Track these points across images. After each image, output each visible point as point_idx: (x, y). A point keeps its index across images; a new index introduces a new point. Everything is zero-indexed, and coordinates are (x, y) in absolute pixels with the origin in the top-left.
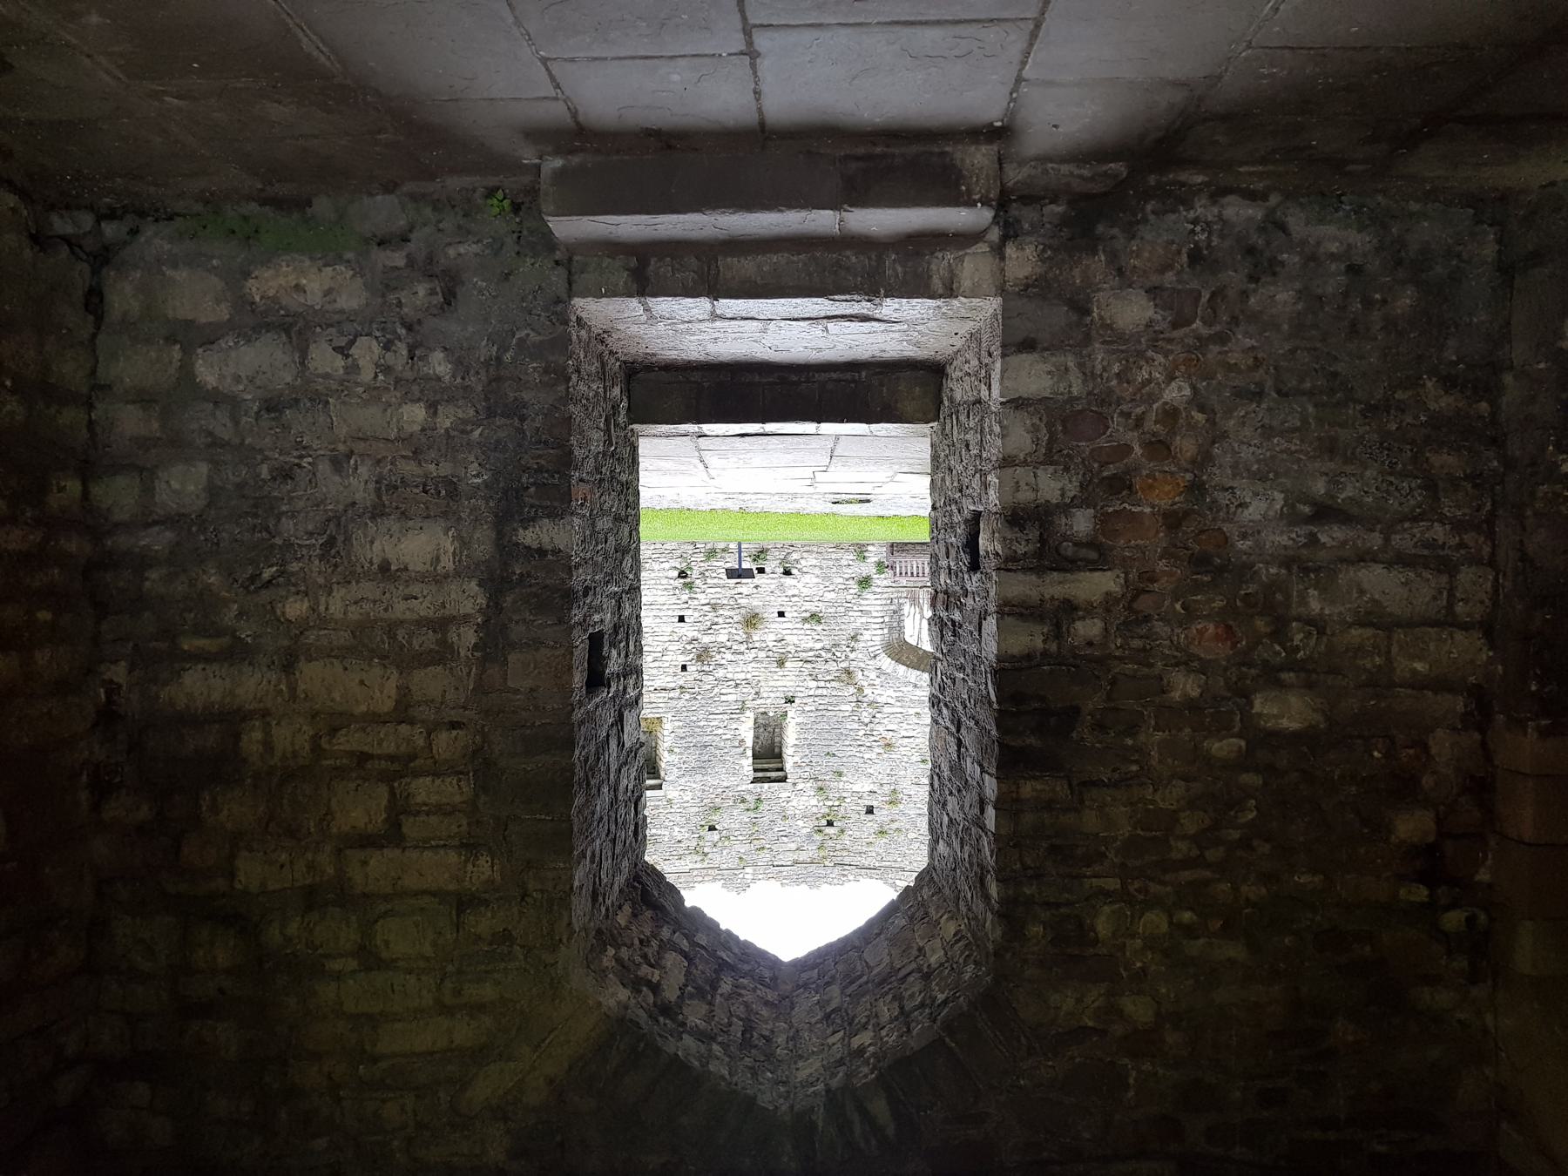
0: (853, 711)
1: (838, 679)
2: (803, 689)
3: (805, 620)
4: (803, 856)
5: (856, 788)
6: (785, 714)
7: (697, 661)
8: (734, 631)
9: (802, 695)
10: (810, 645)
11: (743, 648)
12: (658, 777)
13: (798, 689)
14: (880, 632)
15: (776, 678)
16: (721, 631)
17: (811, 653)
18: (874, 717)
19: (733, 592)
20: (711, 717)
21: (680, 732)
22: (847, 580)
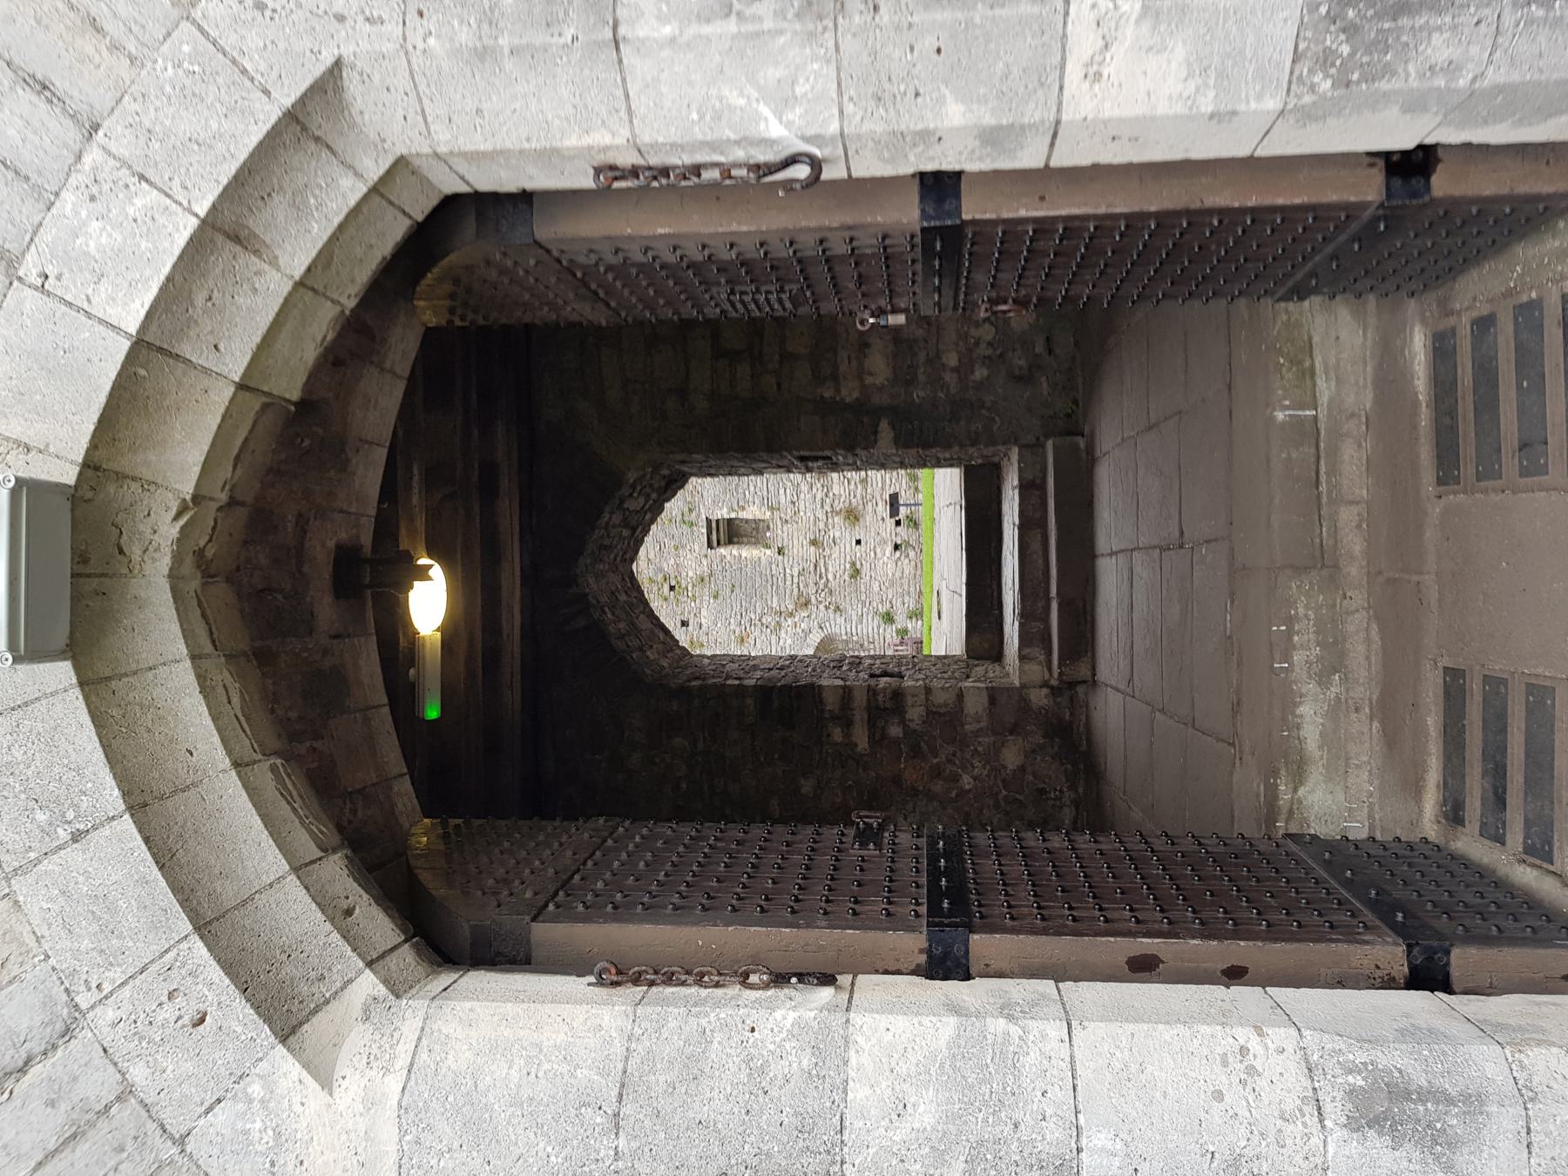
1: (800, 594)
3: (853, 564)
5: (704, 613)
6: (768, 547)
10: (830, 569)
13: (791, 559)
14: (843, 633)
15: (801, 538)
16: (842, 488)
17: (823, 570)
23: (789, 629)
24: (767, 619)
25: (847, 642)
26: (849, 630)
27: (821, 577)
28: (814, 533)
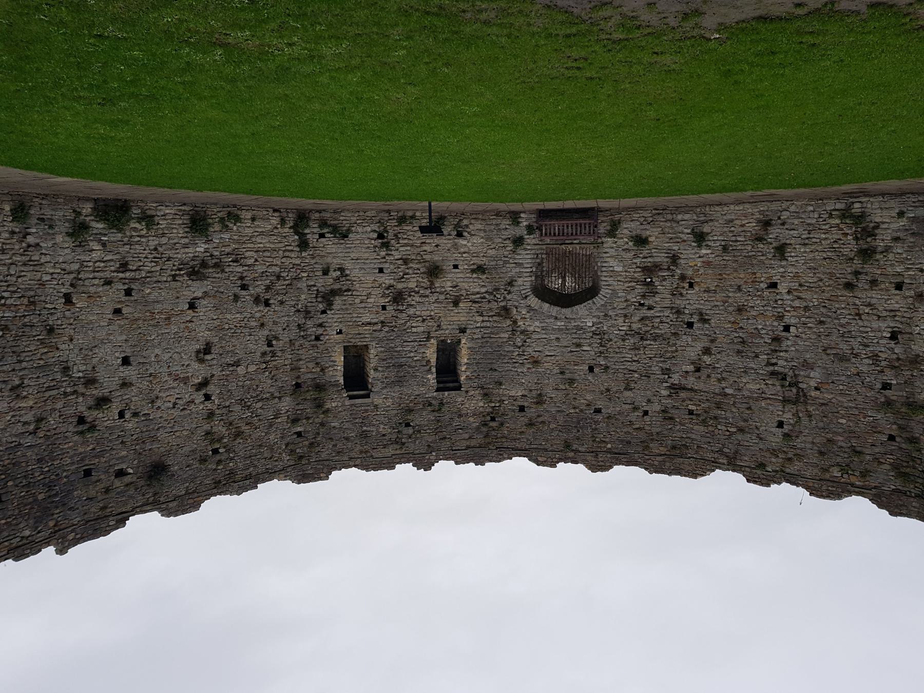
0: (509, 338)
1: (498, 315)
2: (472, 323)
3: (473, 271)
6: (459, 341)
7: (394, 303)
8: (421, 280)
9: (472, 327)
10: (477, 290)
11: (428, 292)
12: (366, 388)
13: (469, 322)
14: (530, 279)
15: (452, 314)
17: (478, 296)
18: (525, 342)
19: (419, 250)
20: (405, 344)
21: (382, 355)
22: (505, 240)
23: (527, 324)
24: (519, 342)
25: (537, 277)
26: (528, 274)
27: (484, 298)
28: (448, 303)
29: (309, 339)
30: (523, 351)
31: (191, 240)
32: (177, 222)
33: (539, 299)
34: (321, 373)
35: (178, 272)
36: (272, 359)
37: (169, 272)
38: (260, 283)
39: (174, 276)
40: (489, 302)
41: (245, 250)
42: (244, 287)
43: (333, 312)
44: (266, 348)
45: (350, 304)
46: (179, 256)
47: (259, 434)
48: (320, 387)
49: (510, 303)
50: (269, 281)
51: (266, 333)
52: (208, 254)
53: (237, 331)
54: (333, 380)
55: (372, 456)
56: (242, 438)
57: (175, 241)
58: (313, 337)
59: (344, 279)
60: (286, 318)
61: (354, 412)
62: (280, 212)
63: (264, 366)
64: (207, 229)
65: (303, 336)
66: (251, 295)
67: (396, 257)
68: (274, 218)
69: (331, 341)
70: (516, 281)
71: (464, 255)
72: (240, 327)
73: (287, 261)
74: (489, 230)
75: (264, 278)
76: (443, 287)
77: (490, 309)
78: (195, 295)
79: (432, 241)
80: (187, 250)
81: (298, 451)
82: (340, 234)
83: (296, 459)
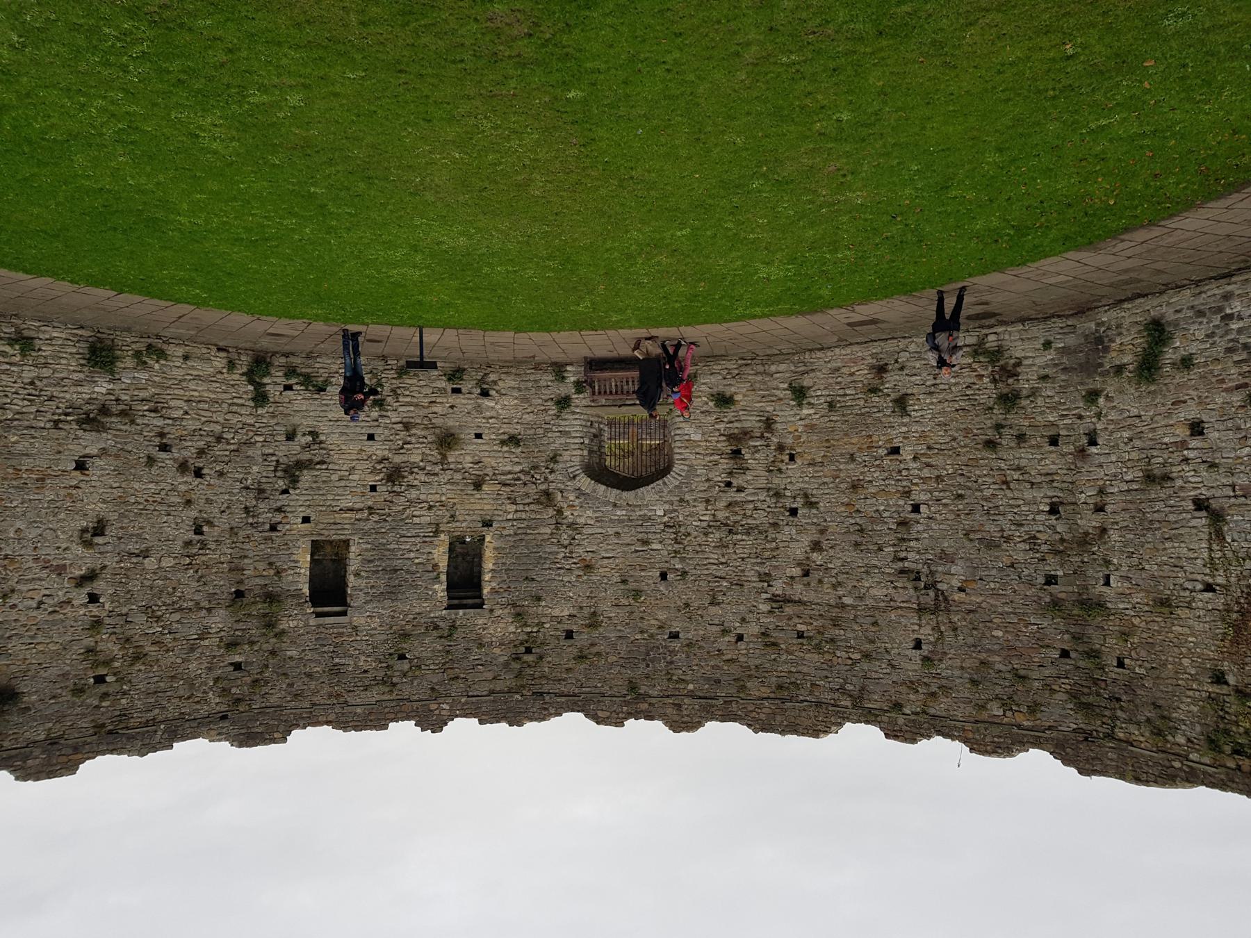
0: (552, 534)
1: (538, 502)
2: (501, 513)
3: (503, 443)
4: (499, 686)
6: (482, 539)
7: (387, 482)
8: (428, 452)
9: (501, 519)
10: (508, 468)
11: (437, 468)
12: (345, 604)
13: (496, 512)
14: (580, 452)
15: (472, 501)
17: (510, 476)
18: (574, 539)
19: (426, 411)
20: (402, 539)
21: (368, 555)
22: (546, 401)
23: (576, 514)
24: (565, 538)
25: (590, 452)
26: (577, 446)
27: (518, 479)
28: (466, 485)
29: (260, 529)
30: (571, 552)
31: (87, 376)
32: (69, 350)
33: (592, 479)
34: (276, 578)
35: (62, 417)
36: (201, 552)
37: (49, 416)
38: (189, 444)
39: (56, 422)
40: (525, 484)
41: (170, 397)
42: (164, 448)
43: (297, 491)
44: (191, 536)
45: (324, 482)
46: (68, 396)
47: (172, 660)
48: (271, 598)
49: (553, 486)
50: (203, 443)
51: (194, 514)
52: (113, 398)
53: (148, 507)
54: (292, 588)
55: (346, 702)
56: (144, 663)
57: (62, 375)
58: (267, 526)
59: (316, 446)
60: (227, 497)
61: (322, 636)
62: (228, 352)
63: (188, 561)
64: (112, 363)
65: (251, 524)
66: (175, 460)
67: (393, 420)
68: (219, 359)
69: (293, 532)
70: (561, 455)
71: (490, 421)
72: (154, 502)
73: (234, 420)
74: (526, 388)
75: (196, 438)
76: (460, 463)
77: (527, 494)
78: (87, 451)
79: (445, 400)
80: (79, 389)
81: (233, 691)
82: (314, 386)
83: (230, 703)
